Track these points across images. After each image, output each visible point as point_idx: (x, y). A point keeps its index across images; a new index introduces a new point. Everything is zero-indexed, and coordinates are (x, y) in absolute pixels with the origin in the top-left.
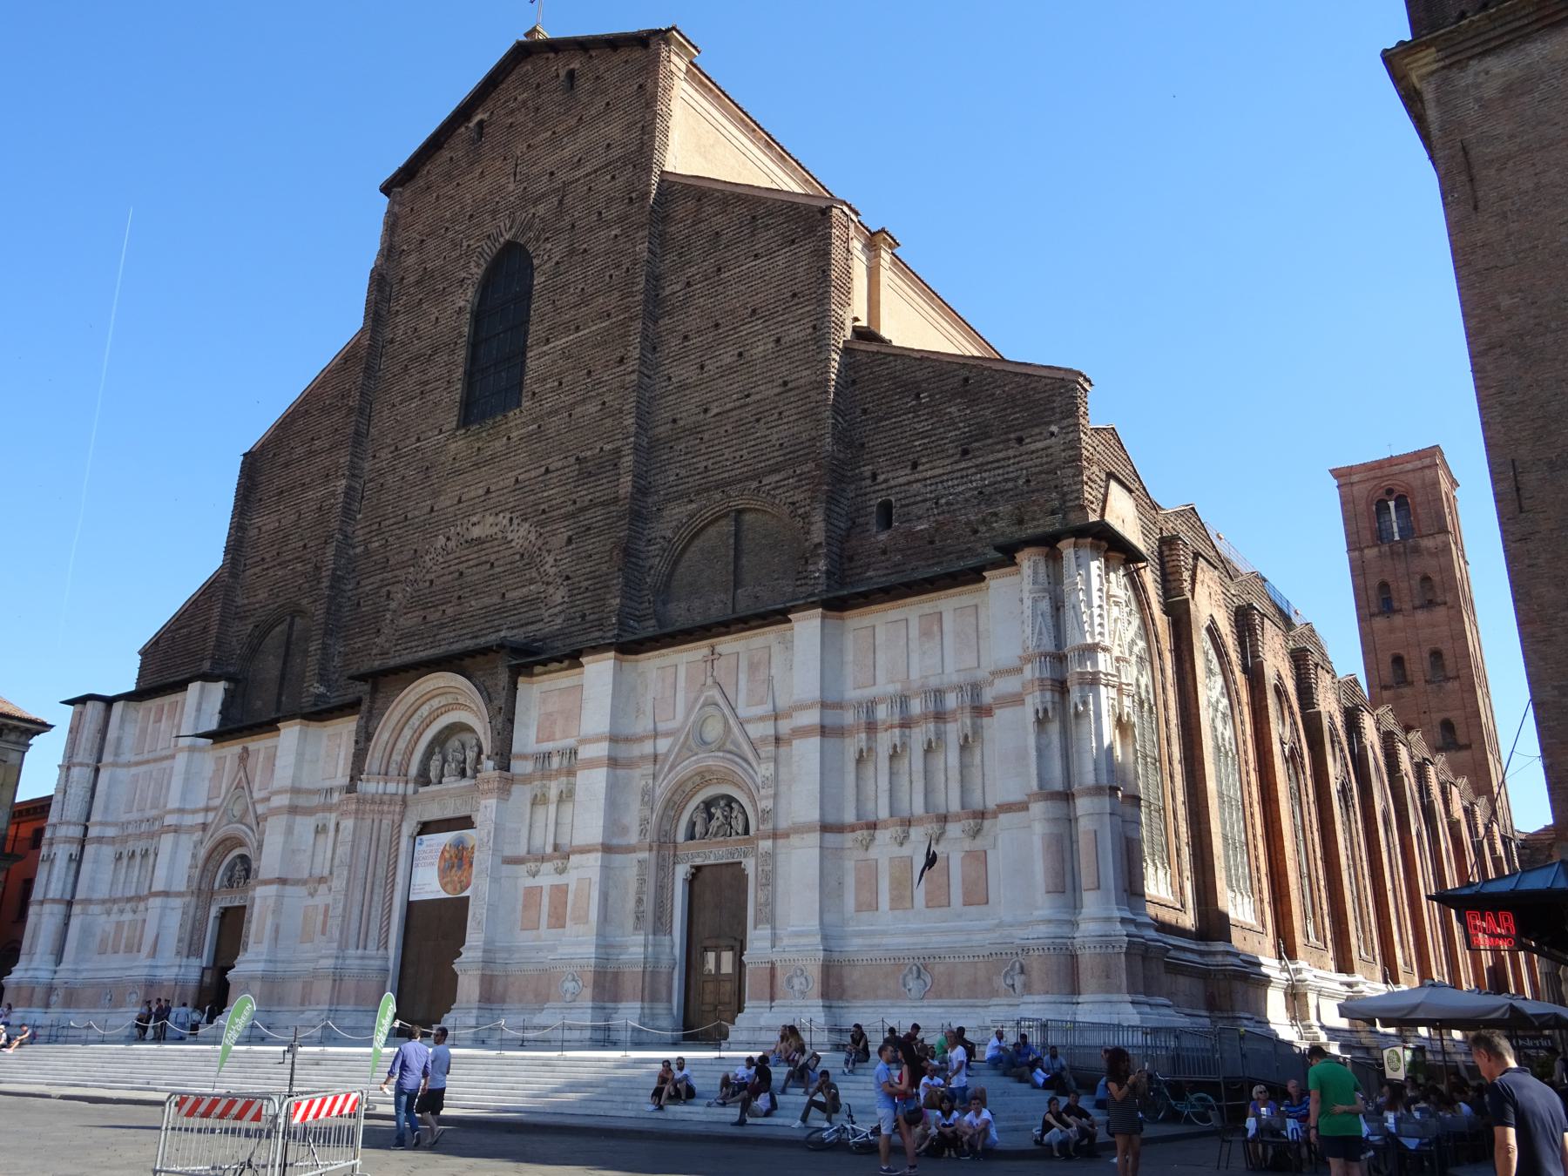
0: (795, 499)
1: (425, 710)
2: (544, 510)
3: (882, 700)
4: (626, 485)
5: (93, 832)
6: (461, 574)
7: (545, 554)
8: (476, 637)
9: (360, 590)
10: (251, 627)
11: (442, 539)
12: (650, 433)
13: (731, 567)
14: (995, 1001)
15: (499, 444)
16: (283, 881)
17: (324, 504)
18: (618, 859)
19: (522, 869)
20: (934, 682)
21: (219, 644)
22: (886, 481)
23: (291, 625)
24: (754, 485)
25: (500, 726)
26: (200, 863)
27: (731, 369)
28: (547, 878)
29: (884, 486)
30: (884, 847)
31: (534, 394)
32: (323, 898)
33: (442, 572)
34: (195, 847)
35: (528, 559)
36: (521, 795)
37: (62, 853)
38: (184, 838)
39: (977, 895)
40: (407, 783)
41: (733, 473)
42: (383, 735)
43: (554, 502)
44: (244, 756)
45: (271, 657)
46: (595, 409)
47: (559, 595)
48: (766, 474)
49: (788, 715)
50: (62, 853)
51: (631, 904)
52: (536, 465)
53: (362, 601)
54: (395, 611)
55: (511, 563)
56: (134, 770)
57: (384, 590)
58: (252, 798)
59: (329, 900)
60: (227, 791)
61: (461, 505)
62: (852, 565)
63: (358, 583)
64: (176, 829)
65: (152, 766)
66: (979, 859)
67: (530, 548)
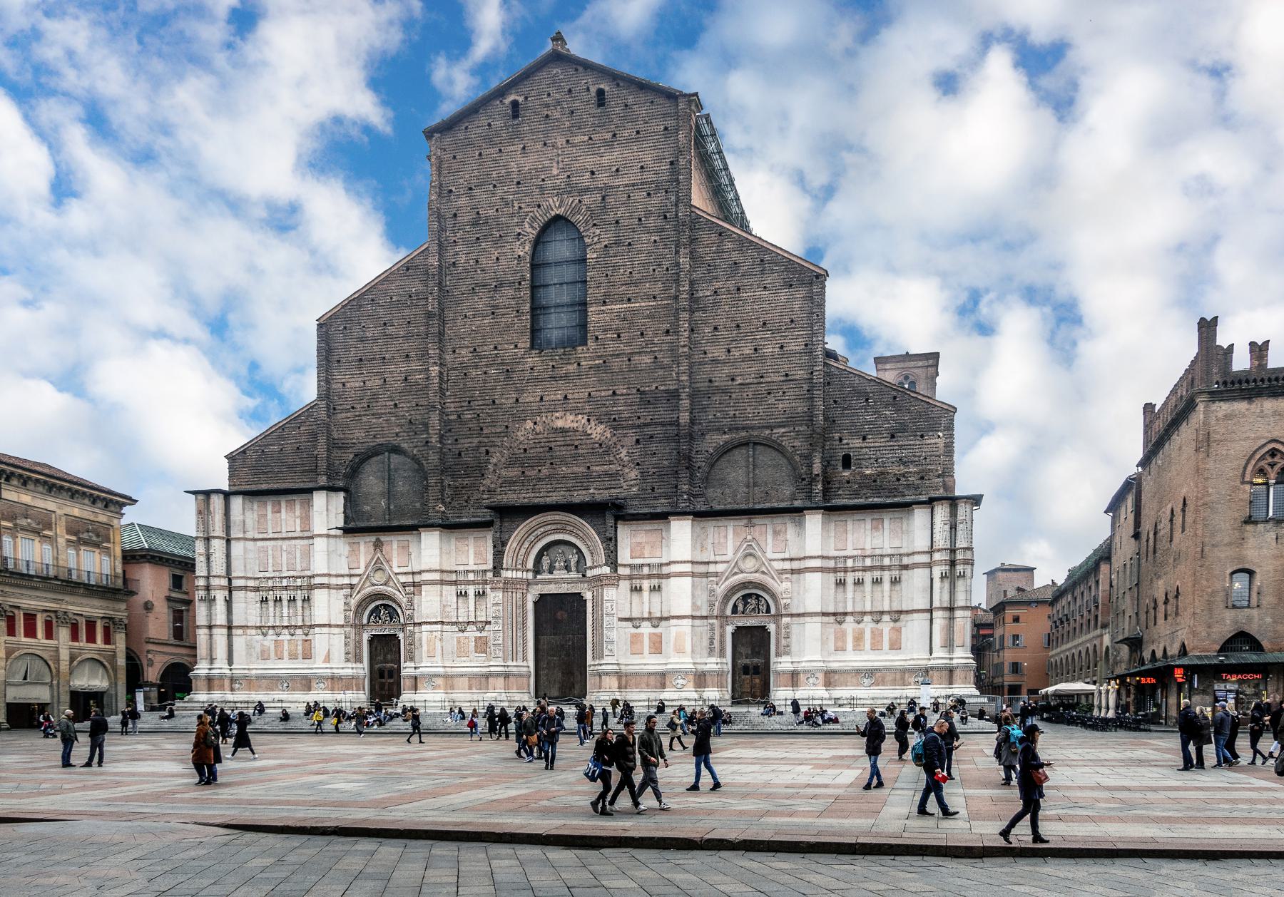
0: (795, 444)
1: (538, 532)
2: (615, 419)
3: (850, 557)
4: (685, 418)
5: (236, 583)
6: (551, 448)
7: (619, 447)
8: (570, 491)
9: (459, 446)
10: (351, 456)
11: (529, 424)
12: (693, 385)
13: (751, 475)
14: (909, 687)
15: (572, 368)
16: (443, 623)
17: (409, 378)
18: (698, 622)
19: (629, 624)
20: (878, 552)
21: (329, 465)
22: (848, 444)
23: (389, 459)
24: (768, 432)
25: (612, 548)
26: (353, 609)
27: (745, 359)
28: (646, 629)
29: (846, 446)
30: (849, 625)
31: (597, 338)
32: (472, 633)
33: (534, 445)
34: (346, 597)
35: (604, 450)
36: (624, 585)
37: (220, 596)
38: (333, 591)
39: (895, 646)
40: (528, 571)
41: (754, 422)
42: (512, 544)
43: (623, 416)
44: (378, 545)
45: (371, 478)
46: (648, 361)
47: (633, 474)
48: (775, 427)
49: (800, 559)
50: (220, 596)
51: (706, 643)
52: (604, 388)
53: (463, 454)
54: (496, 465)
55: (593, 449)
56: (260, 544)
57: (484, 449)
58: (392, 571)
59: (478, 634)
60: (366, 567)
61: (544, 403)
62: (830, 486)
63: (456, 440)
64: (328, 587)
65: (280, 542)
66: (899, 630)
67: (607, 441)
